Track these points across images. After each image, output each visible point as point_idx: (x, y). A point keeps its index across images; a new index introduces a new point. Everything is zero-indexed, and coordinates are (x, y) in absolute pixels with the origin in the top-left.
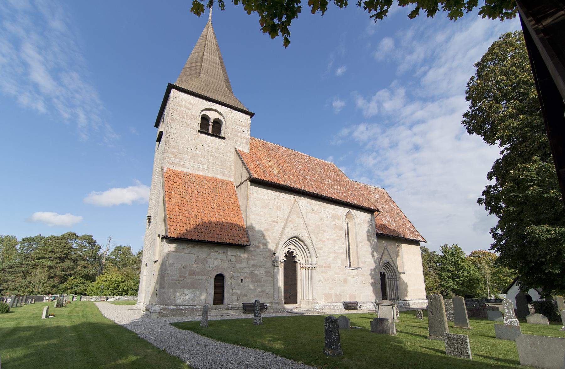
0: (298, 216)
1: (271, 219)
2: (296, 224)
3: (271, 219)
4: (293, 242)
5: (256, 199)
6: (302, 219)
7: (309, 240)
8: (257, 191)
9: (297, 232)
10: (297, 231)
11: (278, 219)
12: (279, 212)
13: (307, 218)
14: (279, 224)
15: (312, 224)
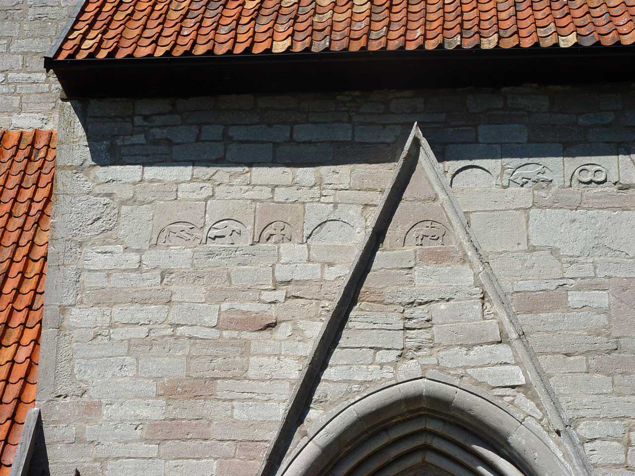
0: (436, 245)
1: (225, 306)
2: (419, 312)
3: (225, 306)
4: (427, 448)
5: (109, 195)
6: (466, 266)
7: (538, 414)
8: (119, 142)
9: (424, 368)
10: (425, 361)
11: (280, 294)
12: (284, 247)
13: (533, 249)
14: (284, 330)
15: (578, 289)
